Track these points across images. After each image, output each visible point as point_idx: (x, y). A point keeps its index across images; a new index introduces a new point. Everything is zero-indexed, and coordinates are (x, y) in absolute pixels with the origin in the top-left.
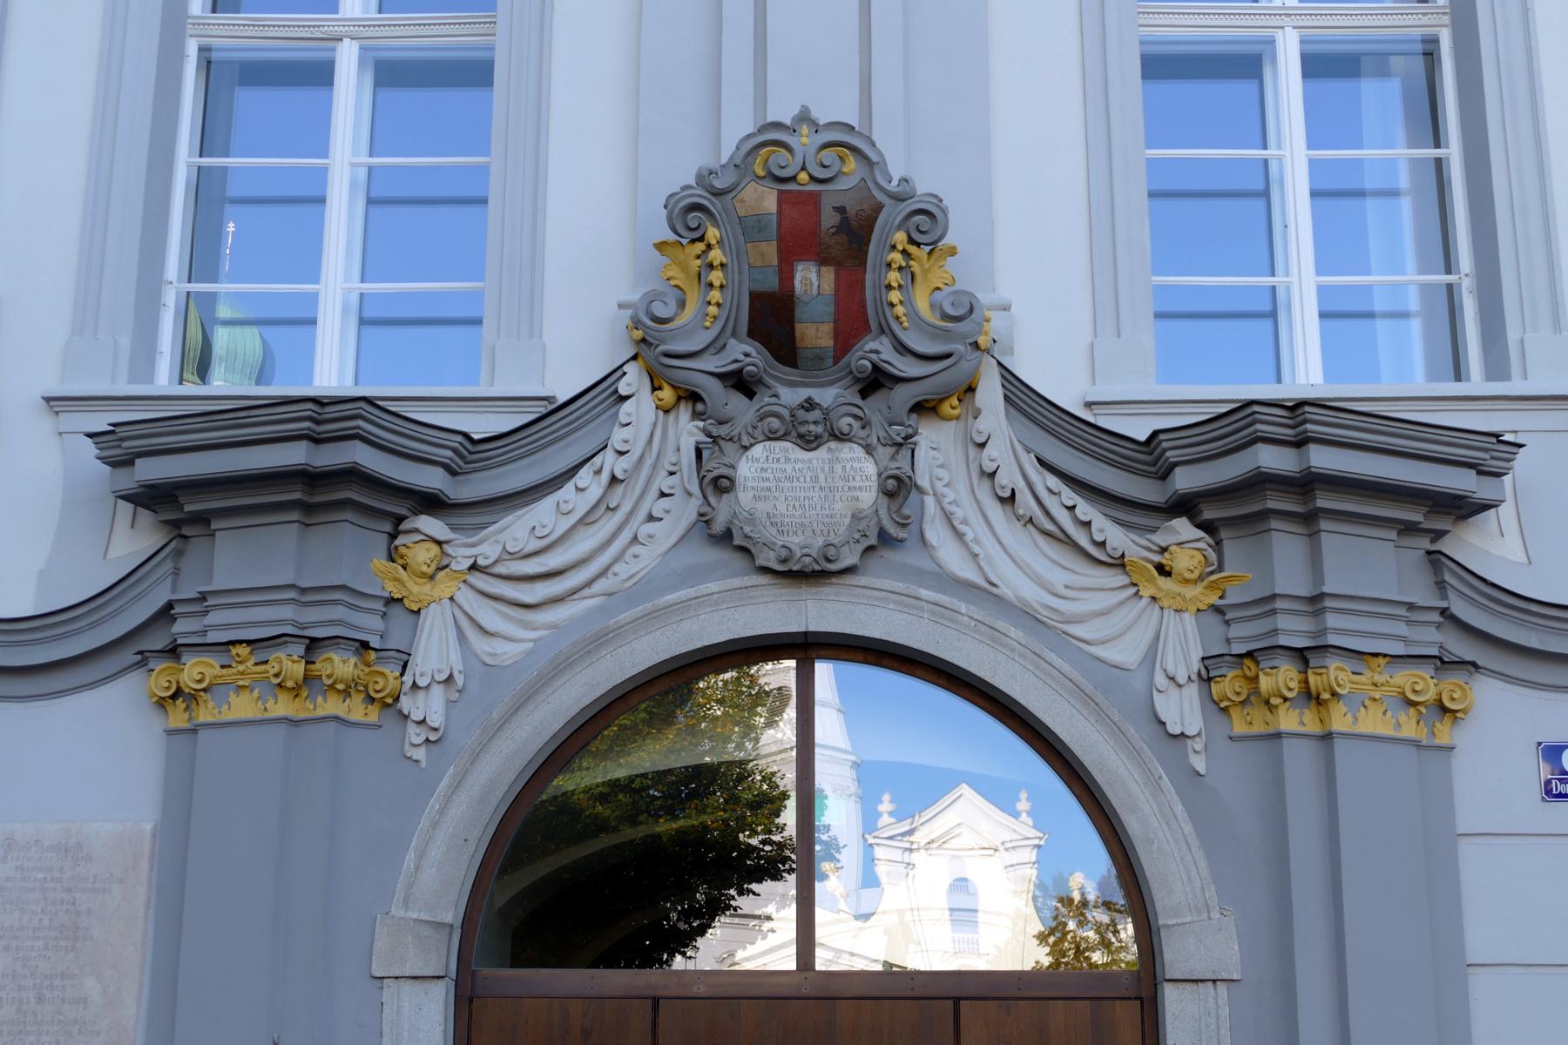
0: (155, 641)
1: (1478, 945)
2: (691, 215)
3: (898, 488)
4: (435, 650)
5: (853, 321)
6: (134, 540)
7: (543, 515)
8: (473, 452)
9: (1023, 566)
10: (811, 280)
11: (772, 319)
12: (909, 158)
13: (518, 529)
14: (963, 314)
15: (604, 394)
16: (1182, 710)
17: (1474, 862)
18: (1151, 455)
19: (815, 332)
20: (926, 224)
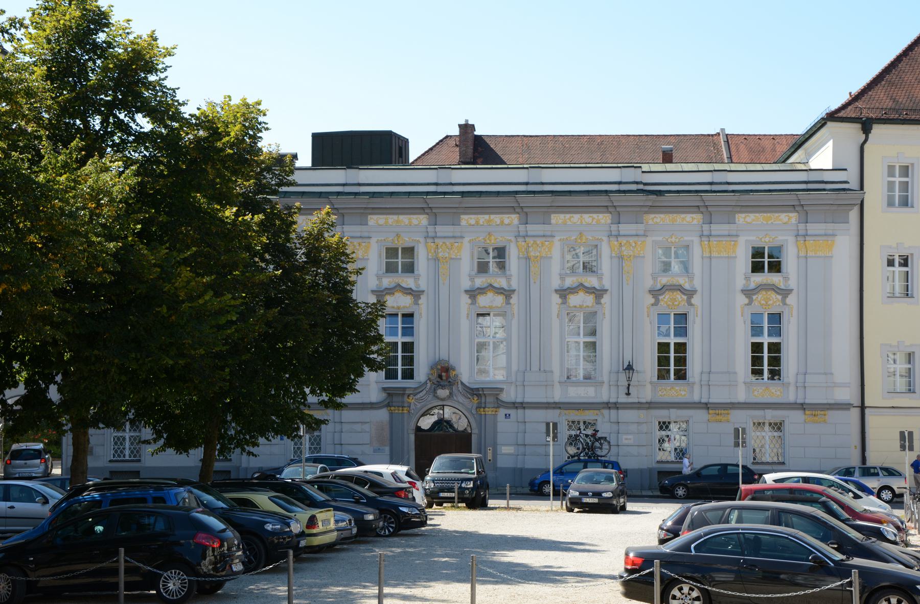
0: (388, 405)
1: (499, 430)
2: (432, 368)
3: (451, 393)
4: (412, 407)
5: (448, 377)
6: (384, 395)
7: (421, 394)
8: (415, 389)
9: (461, 399)
10: (444, 374)
11: (440, 377)
12: (452, 362)
13: (418, 396)
14: (456, 376)
15: (426, 383)
16: (474, 411)
17: (499, 424)
18: (472, 389)
19: (444, 378)
20: (454, 370)
